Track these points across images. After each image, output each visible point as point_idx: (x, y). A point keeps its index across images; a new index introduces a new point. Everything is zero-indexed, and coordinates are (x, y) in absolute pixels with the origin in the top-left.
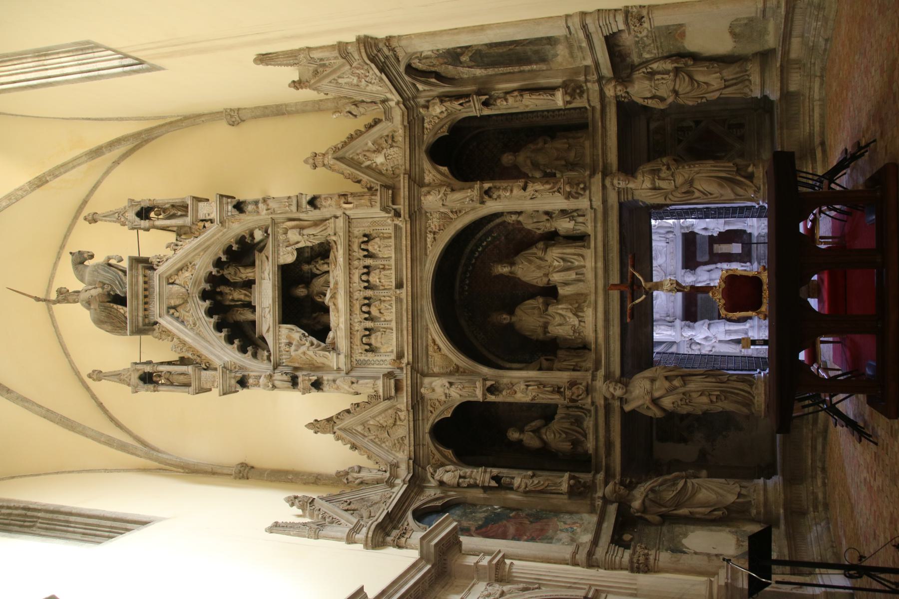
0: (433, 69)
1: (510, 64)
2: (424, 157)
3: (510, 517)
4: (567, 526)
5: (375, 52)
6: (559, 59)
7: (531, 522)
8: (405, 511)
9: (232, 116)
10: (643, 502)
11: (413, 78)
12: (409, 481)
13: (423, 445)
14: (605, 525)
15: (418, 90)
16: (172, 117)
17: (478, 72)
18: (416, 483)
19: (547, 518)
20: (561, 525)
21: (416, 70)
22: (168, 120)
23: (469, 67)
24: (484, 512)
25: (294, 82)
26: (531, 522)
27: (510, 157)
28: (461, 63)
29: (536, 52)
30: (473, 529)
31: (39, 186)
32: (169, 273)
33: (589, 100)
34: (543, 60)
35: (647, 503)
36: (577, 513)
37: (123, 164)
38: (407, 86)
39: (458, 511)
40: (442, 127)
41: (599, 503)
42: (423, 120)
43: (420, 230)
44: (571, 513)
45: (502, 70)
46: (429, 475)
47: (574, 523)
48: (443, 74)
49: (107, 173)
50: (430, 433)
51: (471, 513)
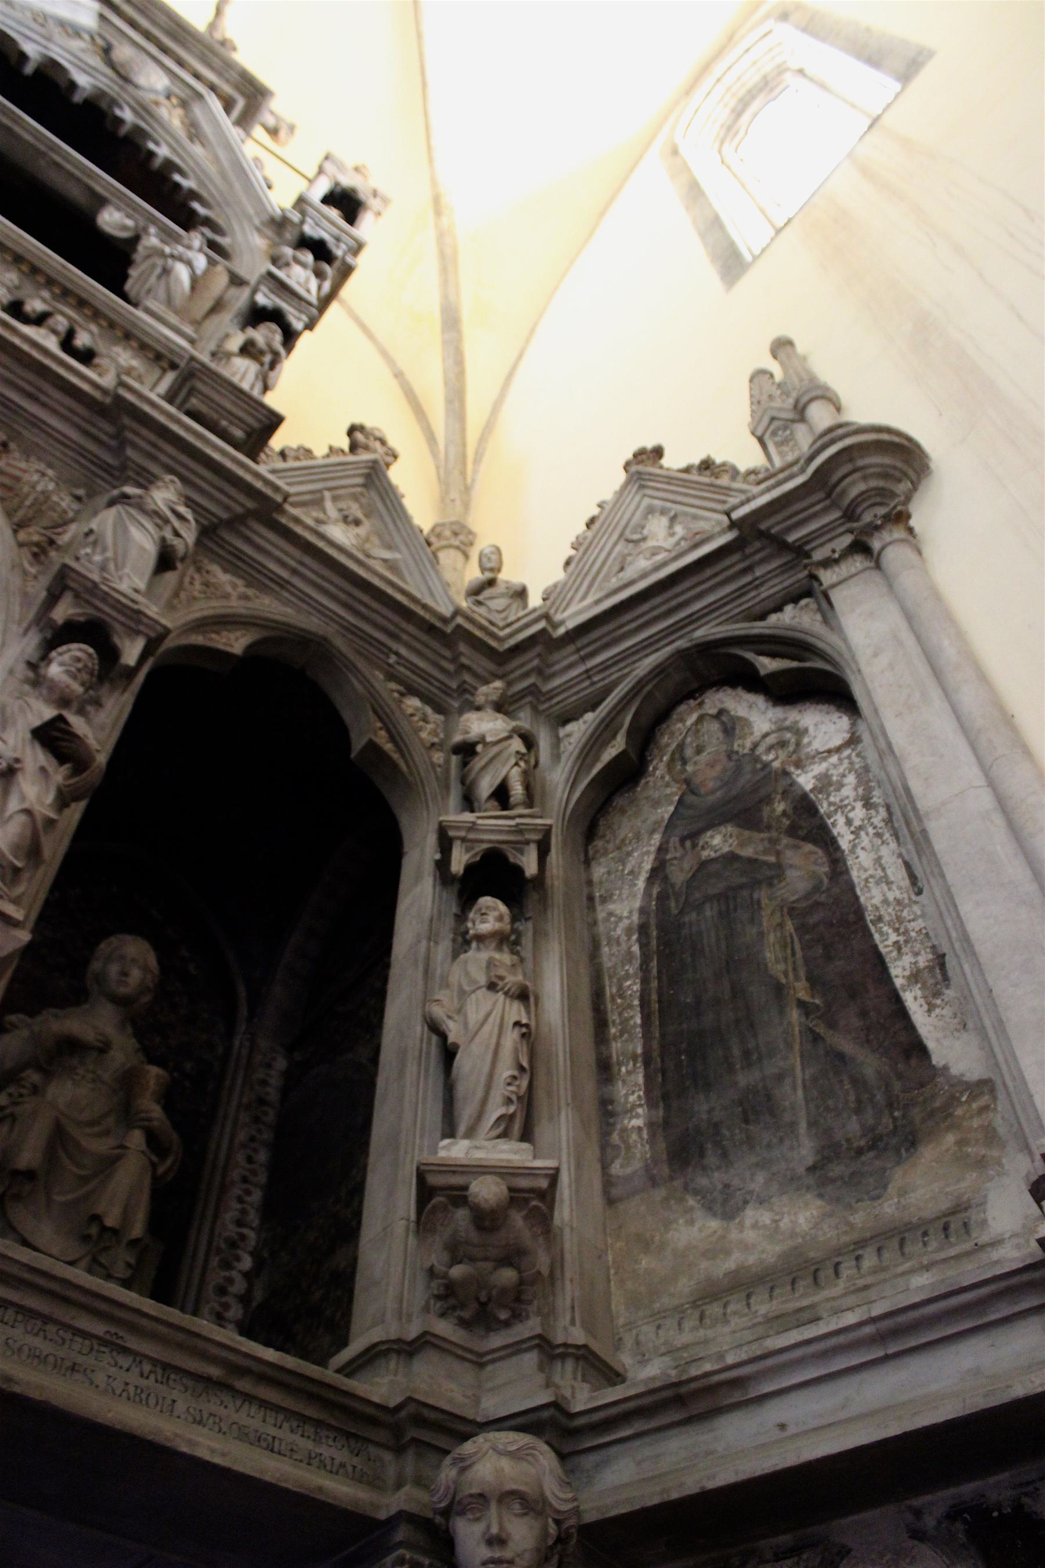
0: (659, 768)
1: (664, 1007)
2: (312, 623)
5: (854, 492)
6: (693, 1230)
9: (456, 534)
11: (640, 684)
15: (566, 720)
16: (475, 471)
17: (625, 905)
21: (664, 716)
22: (470, 466)
23: (658, 872)
25: (658, 452)
27: (136, 975)
28: (693, 836)
29: (758, 1107)
31: (437, 201)
32: (197, 110)
33: (407, 1349)
34: (684, 1150)
37: (394, 383)
38: (604, 667)
40: (392, 738)
42: (439, 709)
43: (36, 423)
45: (627, 986)
48: (619, 801)
49: (384, 354)
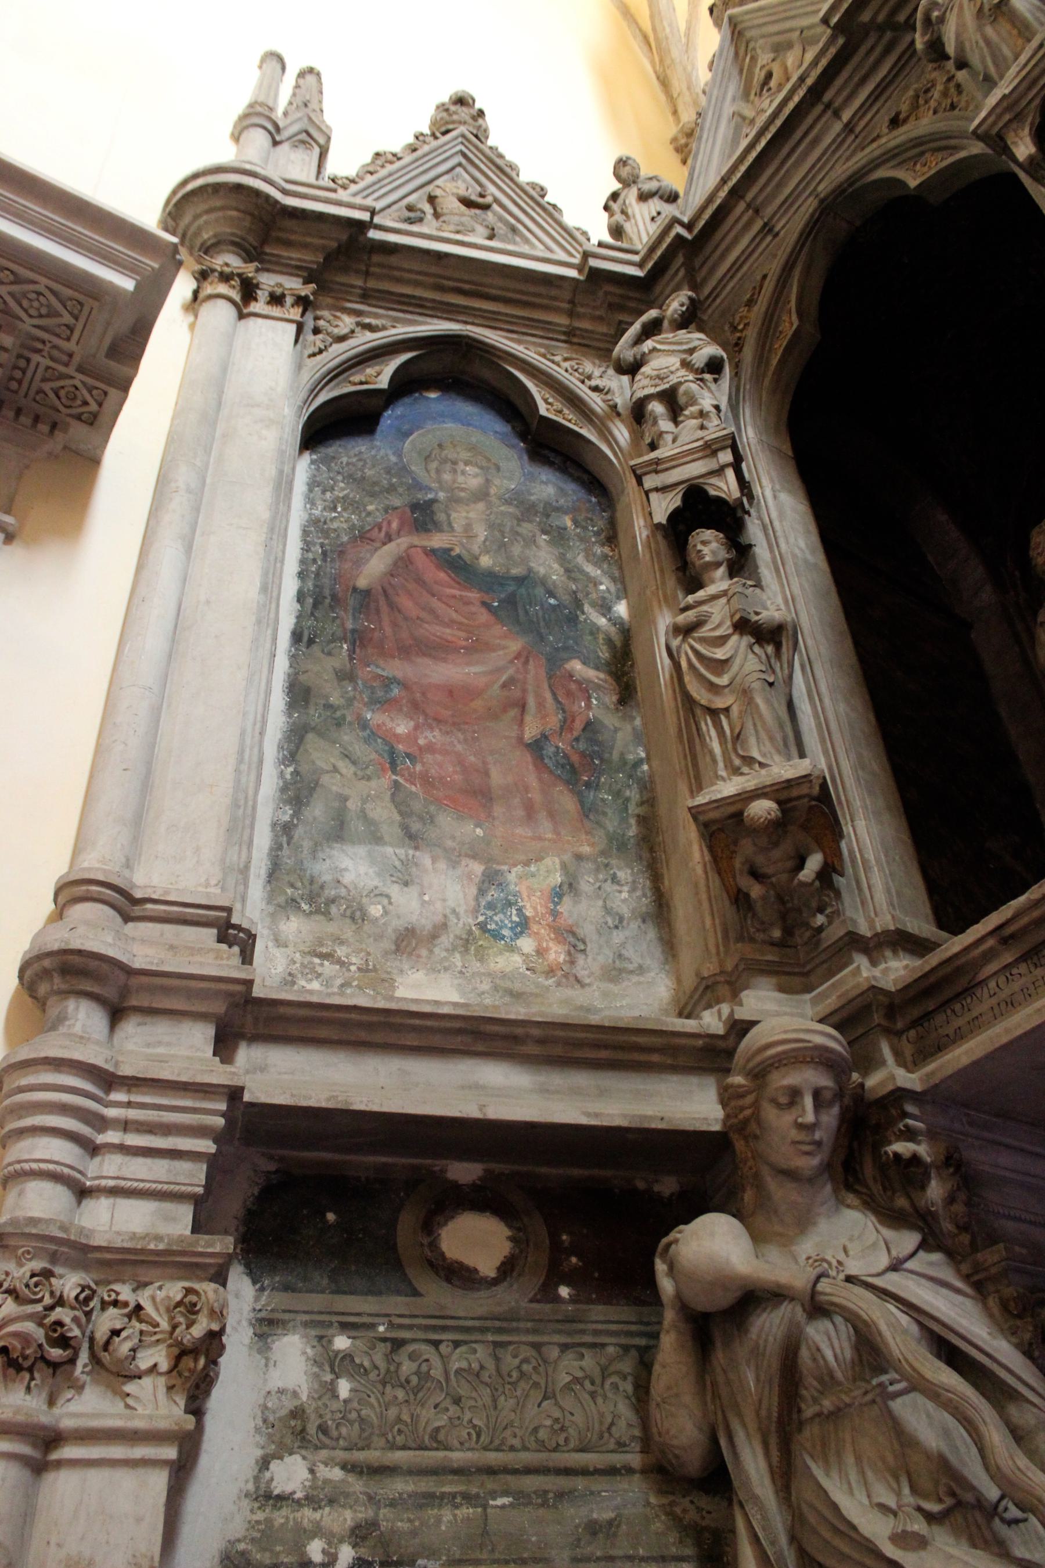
3: (554, 663)
4: (532, 906)
7: (536, 747)
8: (448, 311)
10: (752, 1298)
12: (596, 275)
13: (768, 229)
14: (495, 1074)
18: (603, 302)
19: (588, 811)
20: (533, 883)
24: (570, 571)
26: (536, 747)
30: (438, 541)
35: (769, 1326)
36: (669, 946)
39: (547, 486)
41: (712, 1021)
44: (660, 911)
46: (653, 313)
47: (573, 940)
50: (828, 207)
51: (559, 537)
